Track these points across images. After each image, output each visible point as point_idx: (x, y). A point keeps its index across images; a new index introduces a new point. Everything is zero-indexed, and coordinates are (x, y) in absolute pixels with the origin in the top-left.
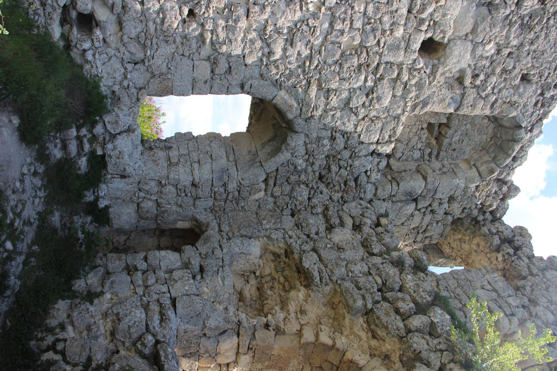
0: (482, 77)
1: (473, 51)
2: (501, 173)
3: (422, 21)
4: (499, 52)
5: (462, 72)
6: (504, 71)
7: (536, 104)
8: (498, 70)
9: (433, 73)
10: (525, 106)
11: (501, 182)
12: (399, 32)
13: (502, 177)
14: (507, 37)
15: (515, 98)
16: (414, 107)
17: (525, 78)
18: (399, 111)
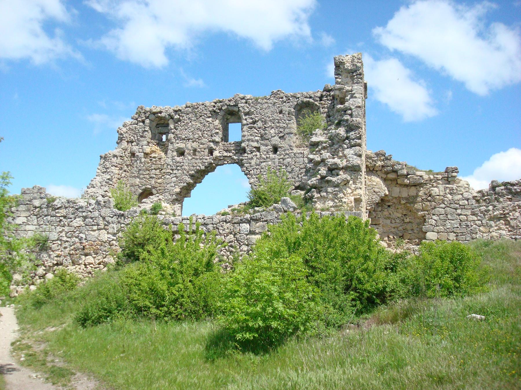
0: (281, 130)
1: (274, 137)
2: (317, 101)
3: (267, 158)
4: (273, 128)
5: (280, 137)
6: (278, 123)
7: (289, 102)
8: (278, 125)
9: (280, 147)
10: (289, 107)
11: (321, 98)
12: (270, 163)
13: (318, 99)
14: (269, 127)
15: (287, 113)
16: (292, 149)
17: (281, 112)
18: (293, 154)
